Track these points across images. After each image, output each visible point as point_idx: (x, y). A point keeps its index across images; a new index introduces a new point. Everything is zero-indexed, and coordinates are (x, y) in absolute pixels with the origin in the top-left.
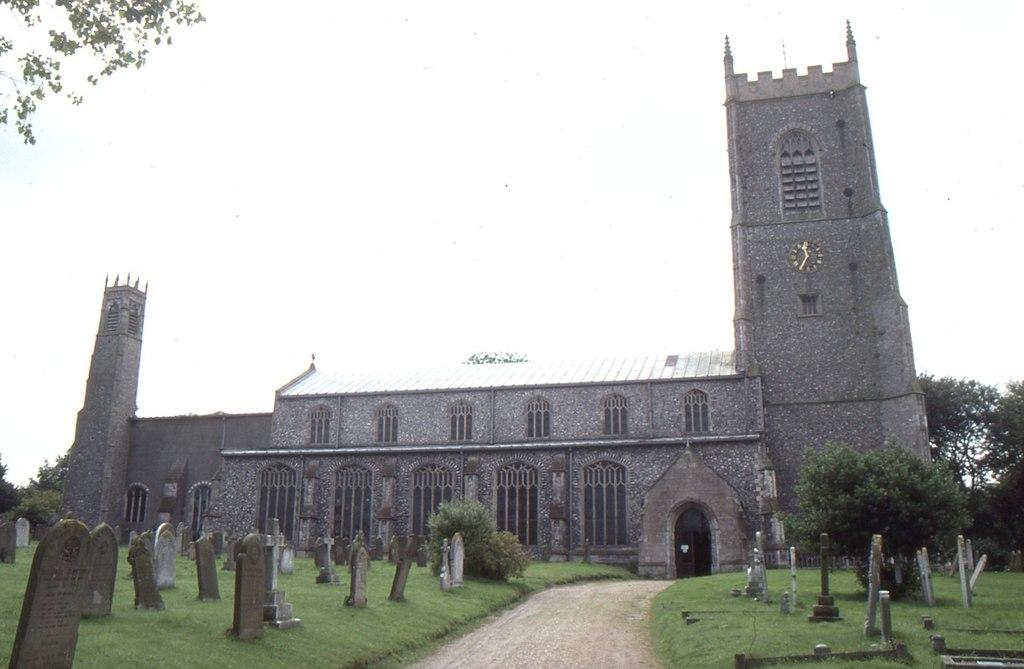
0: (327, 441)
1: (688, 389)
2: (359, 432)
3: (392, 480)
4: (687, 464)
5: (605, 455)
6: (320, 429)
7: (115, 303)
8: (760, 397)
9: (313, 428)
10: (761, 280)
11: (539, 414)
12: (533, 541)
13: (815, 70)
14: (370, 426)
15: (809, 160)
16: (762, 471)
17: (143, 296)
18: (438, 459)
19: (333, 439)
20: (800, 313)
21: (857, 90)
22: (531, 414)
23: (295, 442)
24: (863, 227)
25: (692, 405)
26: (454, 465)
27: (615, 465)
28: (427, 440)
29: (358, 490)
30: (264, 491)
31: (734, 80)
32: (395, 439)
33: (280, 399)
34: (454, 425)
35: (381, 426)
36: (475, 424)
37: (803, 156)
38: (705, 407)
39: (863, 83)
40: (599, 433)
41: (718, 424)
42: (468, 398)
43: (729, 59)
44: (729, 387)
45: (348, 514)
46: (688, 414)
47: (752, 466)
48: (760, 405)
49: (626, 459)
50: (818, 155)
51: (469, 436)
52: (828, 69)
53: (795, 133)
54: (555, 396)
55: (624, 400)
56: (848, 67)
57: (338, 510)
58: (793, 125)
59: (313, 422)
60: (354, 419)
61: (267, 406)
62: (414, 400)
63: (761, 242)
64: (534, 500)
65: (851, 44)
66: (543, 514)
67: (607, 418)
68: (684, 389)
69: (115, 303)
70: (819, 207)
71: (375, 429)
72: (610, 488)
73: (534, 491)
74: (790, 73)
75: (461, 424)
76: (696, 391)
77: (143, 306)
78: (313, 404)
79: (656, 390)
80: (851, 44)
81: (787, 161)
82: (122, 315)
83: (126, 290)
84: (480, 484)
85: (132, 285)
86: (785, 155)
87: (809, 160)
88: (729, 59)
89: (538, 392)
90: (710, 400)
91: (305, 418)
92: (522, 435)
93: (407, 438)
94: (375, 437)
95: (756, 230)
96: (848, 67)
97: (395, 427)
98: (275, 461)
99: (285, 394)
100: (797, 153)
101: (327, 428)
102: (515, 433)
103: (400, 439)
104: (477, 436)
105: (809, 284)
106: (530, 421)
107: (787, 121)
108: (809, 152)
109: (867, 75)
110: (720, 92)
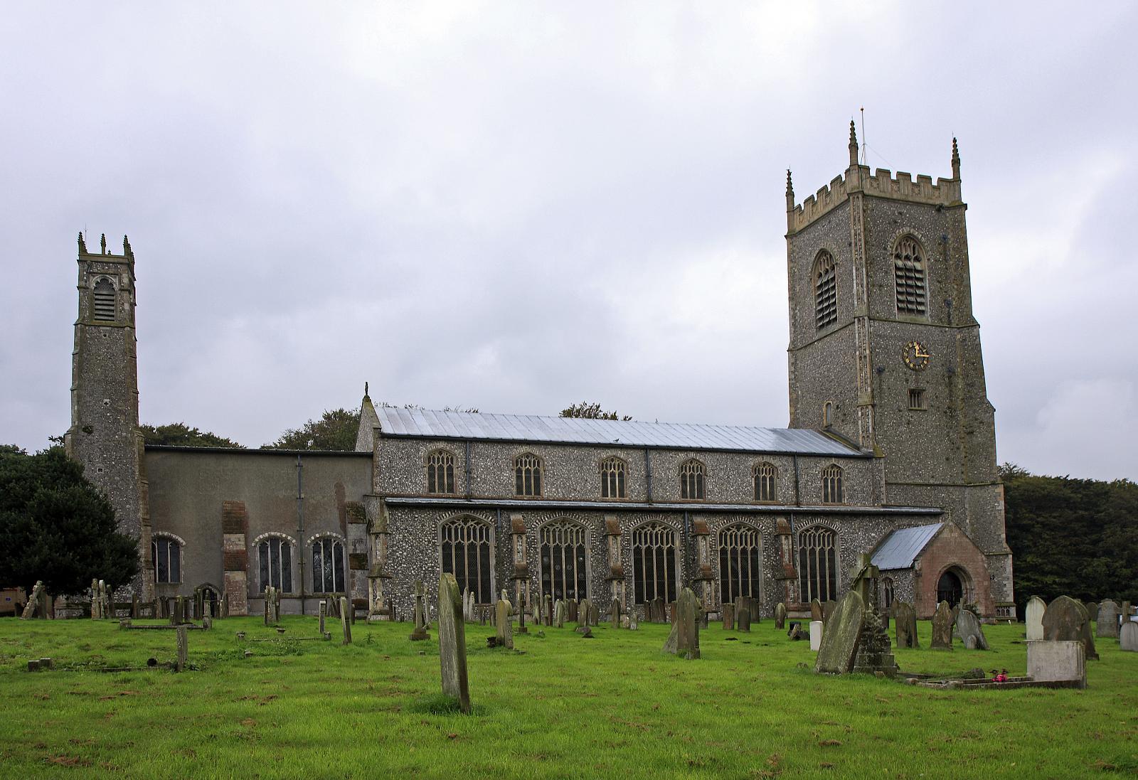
0: (451, 489)
1: (828, 464)
2: (494, 481)
5: (818, 521)
6: (441, 477)
7: (104, 280)
9: (431, 476)
10: (880, 371)
11: (692, 476)
14: (509, 477)
18: (660, 518)
19: (460, 489)
20: (910, 408)
22: (684, 476)
28: (578, 496)
30: (446, 547)
32: (538, 492)
34: (604, 481)
35: (519, 477)
37: (882, 256)
38: (839, 480)
39: (964, 201)
40: (751, 499)
41: (851, 497)
44: (860, 464)
45: (558, 574)
48: (883, 482)
51: (622, 495)
53: (909, 237)
54: (707, 460)
55: (773, 469)
57: (546, 569)
58: (906, 230)
59: (431, 468)
60: (486, 468)
62: (559, 452)
63: (880, 336)
65: (956, 162)
67: (757, 485)
69: (104, 280)
70: (923, 312)
72: (822, 551)
75: (613, 482)
78: (432, 446)
80: (956, 162)
86: (898, 257)
89: (692, 455)
91: (420, 463)
93: (551, 493)
94: (514, 490)
95: (876, 324)
97: (537, 480)
98: (461, 514)
100: (907, 258)
101: (451, 475)
102: (669, 493)
105: (917, 381)
106: (684, 482)
108: (917, 259)
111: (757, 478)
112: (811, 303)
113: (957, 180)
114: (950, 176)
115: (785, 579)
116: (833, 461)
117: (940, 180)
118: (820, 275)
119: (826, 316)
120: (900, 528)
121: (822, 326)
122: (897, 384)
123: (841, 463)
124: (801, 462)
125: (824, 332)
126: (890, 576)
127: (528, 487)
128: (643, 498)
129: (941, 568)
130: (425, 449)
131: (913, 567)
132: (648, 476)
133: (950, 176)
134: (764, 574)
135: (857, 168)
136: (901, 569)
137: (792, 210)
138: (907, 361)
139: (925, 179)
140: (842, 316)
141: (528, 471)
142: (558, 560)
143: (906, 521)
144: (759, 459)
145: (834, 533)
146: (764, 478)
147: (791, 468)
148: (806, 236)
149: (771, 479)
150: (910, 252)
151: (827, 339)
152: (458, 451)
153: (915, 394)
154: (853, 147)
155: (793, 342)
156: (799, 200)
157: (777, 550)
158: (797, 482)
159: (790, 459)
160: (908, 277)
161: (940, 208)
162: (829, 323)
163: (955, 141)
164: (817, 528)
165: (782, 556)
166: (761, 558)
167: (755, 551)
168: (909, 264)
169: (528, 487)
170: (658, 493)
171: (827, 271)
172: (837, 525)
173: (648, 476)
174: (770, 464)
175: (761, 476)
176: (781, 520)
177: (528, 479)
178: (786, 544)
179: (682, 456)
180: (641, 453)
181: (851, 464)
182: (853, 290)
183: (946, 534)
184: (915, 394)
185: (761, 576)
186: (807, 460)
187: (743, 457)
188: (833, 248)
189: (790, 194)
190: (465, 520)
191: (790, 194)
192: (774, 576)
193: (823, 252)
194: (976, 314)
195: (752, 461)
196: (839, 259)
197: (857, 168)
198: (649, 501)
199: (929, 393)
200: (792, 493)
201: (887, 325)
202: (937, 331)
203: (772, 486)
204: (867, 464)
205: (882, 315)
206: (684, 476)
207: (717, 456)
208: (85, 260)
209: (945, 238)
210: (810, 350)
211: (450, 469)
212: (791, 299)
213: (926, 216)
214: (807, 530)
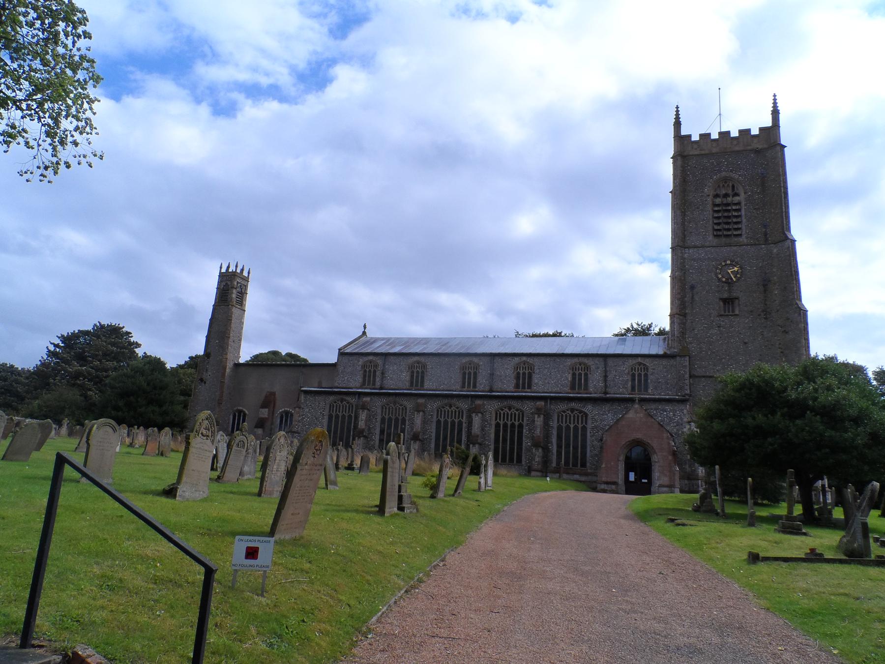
0: (374, 384)
1: (634, 362)
2: (397, 378)
3: (421, 413)
4: (635, 414)
5: (573, 405)
6: (369, 377)
8: (687, 370)
9: (365, 376)
12: (519, 461)
13: (745, 133)
14: (405, 376)
15: (737, 199)
16: (689, 422)
17: (247, 279)
18: (454, 401)
19: (378, 384)
20: (723, 313)
21: (778, 148)
23: (351, 385)
24: (775, 251)
25: (637, 373)
26: (464, 405)
27: (581, 412)
29: (397, 420)
31: (681, 140)
33: (342, 354)
34: (464, 378)
35: (412, 376)
36: (479, 379)
38: (646, 375)
39: (783, 142)
40: (567, 389)
41: (655, 388)
42: (476, 360)
43: (677, 124)
44: (664, 362)
46: (633, 380)
47: (681, 419)
48: (687, 376)
49: (588, 408)
50: (742, 195)
51: (475, 386)
52: (755, 132)
53: (725, 180)
54: (536, 360)
55: (587, 368)
56: (771, 133)
58: (724, 174)
59: (365, 371)
61: (332, 359)
63: (694, 260)
64: (520, 433)
65: (775, 113)
66: (527, 443)
68: (631, 362)
71: (408, 378)
72: (576, 428)
73: (521, 426)
74: (724, 135)
75: (469, 378)
76: (640, 364)
77: (246, 286)
78: (366, 359)
79: (610, 362)
80: (775, 113)
81: (718, 201)
82: (231, 290)
83: (234, 274)
84: (484, 420)
85: (238, 271)
86: (717, 196)
87: (737, 199)
88: (677, 124)
89: (524, 358)
90: (650, 370)
91: (359, 368)
92: (511, 388)
93: (430, 385)
94: (408, 384)
95: (691, 251)
96: (771, 133)
97: (423, 378)
99: (348, 350)
102: (506, 384)
103: (426, 387)
104: (480, 387)
107: (720, 171)
108: (737, 195)
109: (785, 138)
110: (669, 148)
116: (639, 360)
117: (761, 129)
123: (647, 362)
127: (417, 382)
128: (487, 388)
130: (361, 361)
132: (492, 374)
138: (720, 276)
141: (418, 372)
142: (389, 427)
149: (586, 375)
150: (730, 192)
152: (380, 361)
153: (729, 302)
158: (606, 377)
159: (601, 359)
161: (757, 152)
163: (775, 96)
168: (729, 199)
169: (417, 382)
170: (498, 385)
173: (492, 374)
174: (585, 364)
176: (541, 404)
177: (417, 377)
179: (517, 359)
180: (488, 359)
181: (657, 362)
190: (342, 400)
198: (491, 391)
200: (602, 384)
201: (701, 251)
203: (586, 380)
204: (672, 361)
207: (543, 359)
208: (222, 275)
211: (375, 372)
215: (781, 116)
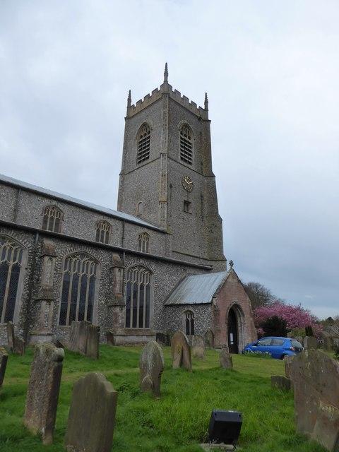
10: (171, 186)
11: (52, 219)
27: (147, 269)
43: (166, 74)
44: (159, 235)
53: (186, 126)
54: (66, 210)
55: (109, 226)
58: (186, 122)
65: (206, 102)
67: (98, 235)
80: (206, 102)
89: (54, 203)
111: (98, 231)
112: (135, 151)
113: (206, 110)
114: (204, 108)
115: (115, 306)
118: (142, 137)
119: (143, 156)
120: (189, 274)
121: (140, 162)
122: (180, 197)
123: (150, 232)
124: (127, 226)
125: (141, 165)
126: (191, 309)
129: (228, 306)
131: (211, 303)
133: (204, 108)
134: (98, 300)
135: (166, 85)
136: (202, 304)
137: (130, 107)
139: (193, 104)
140: (153, 155)
143: (192, 271)
144: (101, 218)
145: (151, 272)
146: (103, 232)
147: (120, 229)
148: (135, 118)
149: (107, 233)
151: (143, 168)
154: (166, 74)
155: (123, 170)
156: (134, 102)
157: (111, 280)
160: (186, 145)
161: (200, 119)
162: (144, 160)
164: (140, 266)
165: (114, 286)
166: (97, 286)
167: (93, 279)
171: (145, 135)
172: (153, 267)
174: (108, 223)
175: (101, 230)
176: (116, 256)
178: (118, 275)
182: (159, 143)
183: (230, 280)
184: (187, 203)
185: (96, 303)
186: (131, 226)
187: (91, 214)
188: (150, 122)
189: (129, 100)
191: (129, 100)
192: (106, 303)
193: (144, 125)
194: (215, 170)
195: (98, 218)
196: (153, 127)
197: (166, 85)
199: (193, 205)
201: (175, 163)
202: (197, 175)
205: (174, 158)
206: (46, 217)
207: (73, 208)
209: (201, 133)
210: (132, 174)
212: (124, 148)
213: (195, 120)
214: (134, 268)
215: (209, 105)
